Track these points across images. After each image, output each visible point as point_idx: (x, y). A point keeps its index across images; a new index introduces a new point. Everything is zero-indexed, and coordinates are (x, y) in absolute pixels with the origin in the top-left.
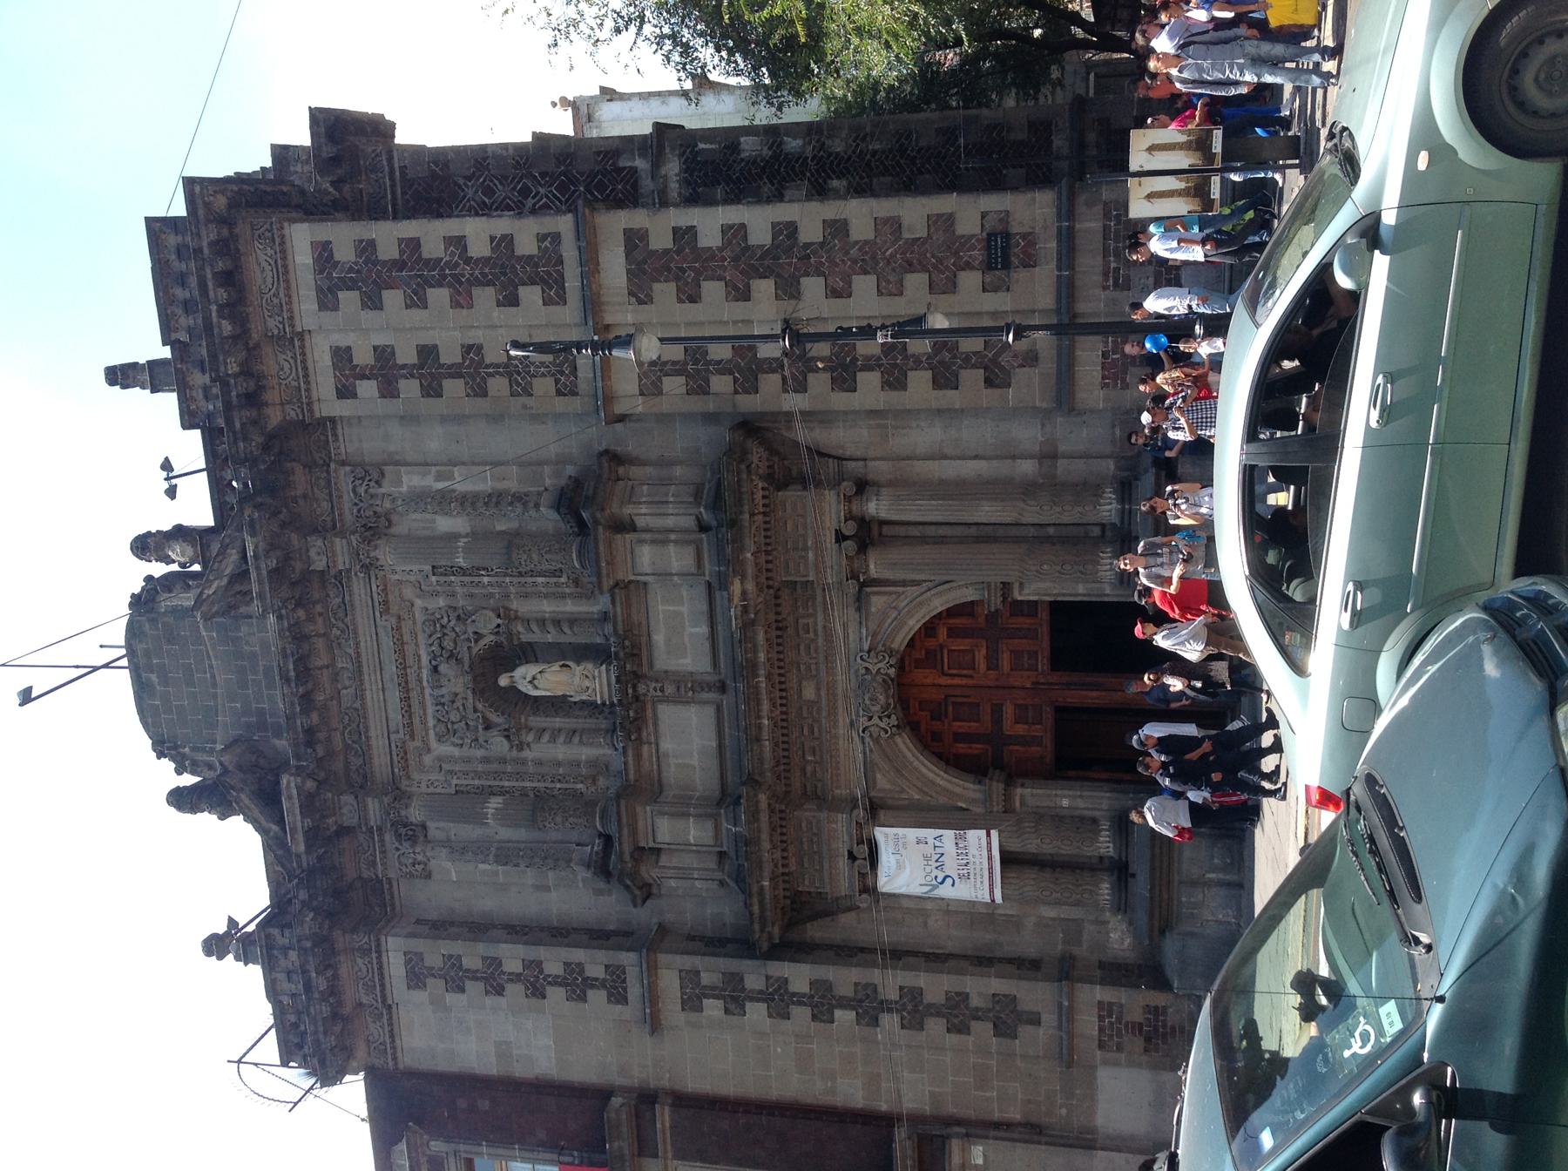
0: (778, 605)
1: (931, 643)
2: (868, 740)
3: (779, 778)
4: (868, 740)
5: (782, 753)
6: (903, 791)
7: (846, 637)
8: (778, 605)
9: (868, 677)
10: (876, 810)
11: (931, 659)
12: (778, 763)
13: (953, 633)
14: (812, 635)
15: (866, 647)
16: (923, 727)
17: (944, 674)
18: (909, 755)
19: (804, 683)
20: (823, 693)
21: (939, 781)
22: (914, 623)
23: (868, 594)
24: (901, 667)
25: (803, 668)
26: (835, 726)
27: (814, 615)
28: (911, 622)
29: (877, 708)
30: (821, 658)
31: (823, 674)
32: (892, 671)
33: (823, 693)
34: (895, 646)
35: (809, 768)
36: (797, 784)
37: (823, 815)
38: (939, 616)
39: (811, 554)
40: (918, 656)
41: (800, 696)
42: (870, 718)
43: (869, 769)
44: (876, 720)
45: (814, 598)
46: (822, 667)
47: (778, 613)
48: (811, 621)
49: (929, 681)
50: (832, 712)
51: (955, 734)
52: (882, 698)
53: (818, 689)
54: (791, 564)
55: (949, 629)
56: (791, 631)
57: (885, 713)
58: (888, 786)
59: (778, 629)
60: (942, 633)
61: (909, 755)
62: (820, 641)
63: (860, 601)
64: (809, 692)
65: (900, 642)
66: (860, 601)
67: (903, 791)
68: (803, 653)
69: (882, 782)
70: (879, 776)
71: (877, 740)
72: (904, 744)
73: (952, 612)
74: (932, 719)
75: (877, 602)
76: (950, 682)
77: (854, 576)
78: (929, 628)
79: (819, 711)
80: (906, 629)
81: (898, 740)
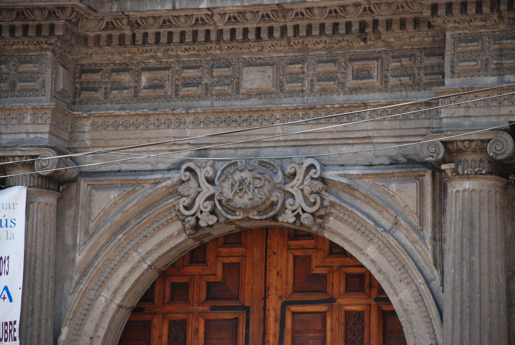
0: (403, 24)
1: (337, 285)
2: (175, 176)
3: (110, 25)
4: (175, 176)
5: (151, 31)
6: (88, 234)
7: (346, 141)
8: (403, 24)
9: (279, 178)
10: (57, 185)
11: (309, 283)
12: (134, 25)
13: (354, 322)
14: (351, 82)
15: (331, 174)
16: (195, 269)
17: (285, 305)
18: (150, 245)
19: (269, 71)
20: (254, 103)
21: (106, 295)
22: (370, 256)
23: (419, 177)
24: (296, 234)
25: (296, 68)
26: (197, 124)
27: (385, 87)
28: (371, 251)
29: (228, 193)
30: (311, 100)
31: (287, 102)
32: (288, 218)
33: (254, 103)
34: (332, 222)
35: (126, 78)
36: (98, 56)
37: (46, 101)
38: (382, 298)
39: (491, 80)
40: (315, 262)
41: (250, 64)
42: (211, 181)
43: (127, 178)
44: (207, 190)
45: (416, 85)
46: (298, 101)
47: (389, 24)
48: (375, 82)
49: (273, 278)
50: (224, 118)
51: (183, 325)
52: (243, 201)
53: (260, 94)
54: (474, 46)
55: (360, 315)
56: (358, 47)
57: (219, 205)
58: (96, 211)
59: (363, 25)
60: (353, 304)
61: (150, 245)
62: (340, 98)
63: (408, 165)
64: (254, 79)
65: (338, 231)
66: (408, 165)
67: (88, 234)
68: (321, 68)
69: (103, 201)
70: (113, 194)
71: (173, 192)
72: (168, 238)
73: (389, 318)
74: (210, 285)
75: (405, 194)
76: (272, 316)
77: (452, 151)
78: (361, 281)
79: (220, 96)
80: (357, 239)
81: (177, 226)
